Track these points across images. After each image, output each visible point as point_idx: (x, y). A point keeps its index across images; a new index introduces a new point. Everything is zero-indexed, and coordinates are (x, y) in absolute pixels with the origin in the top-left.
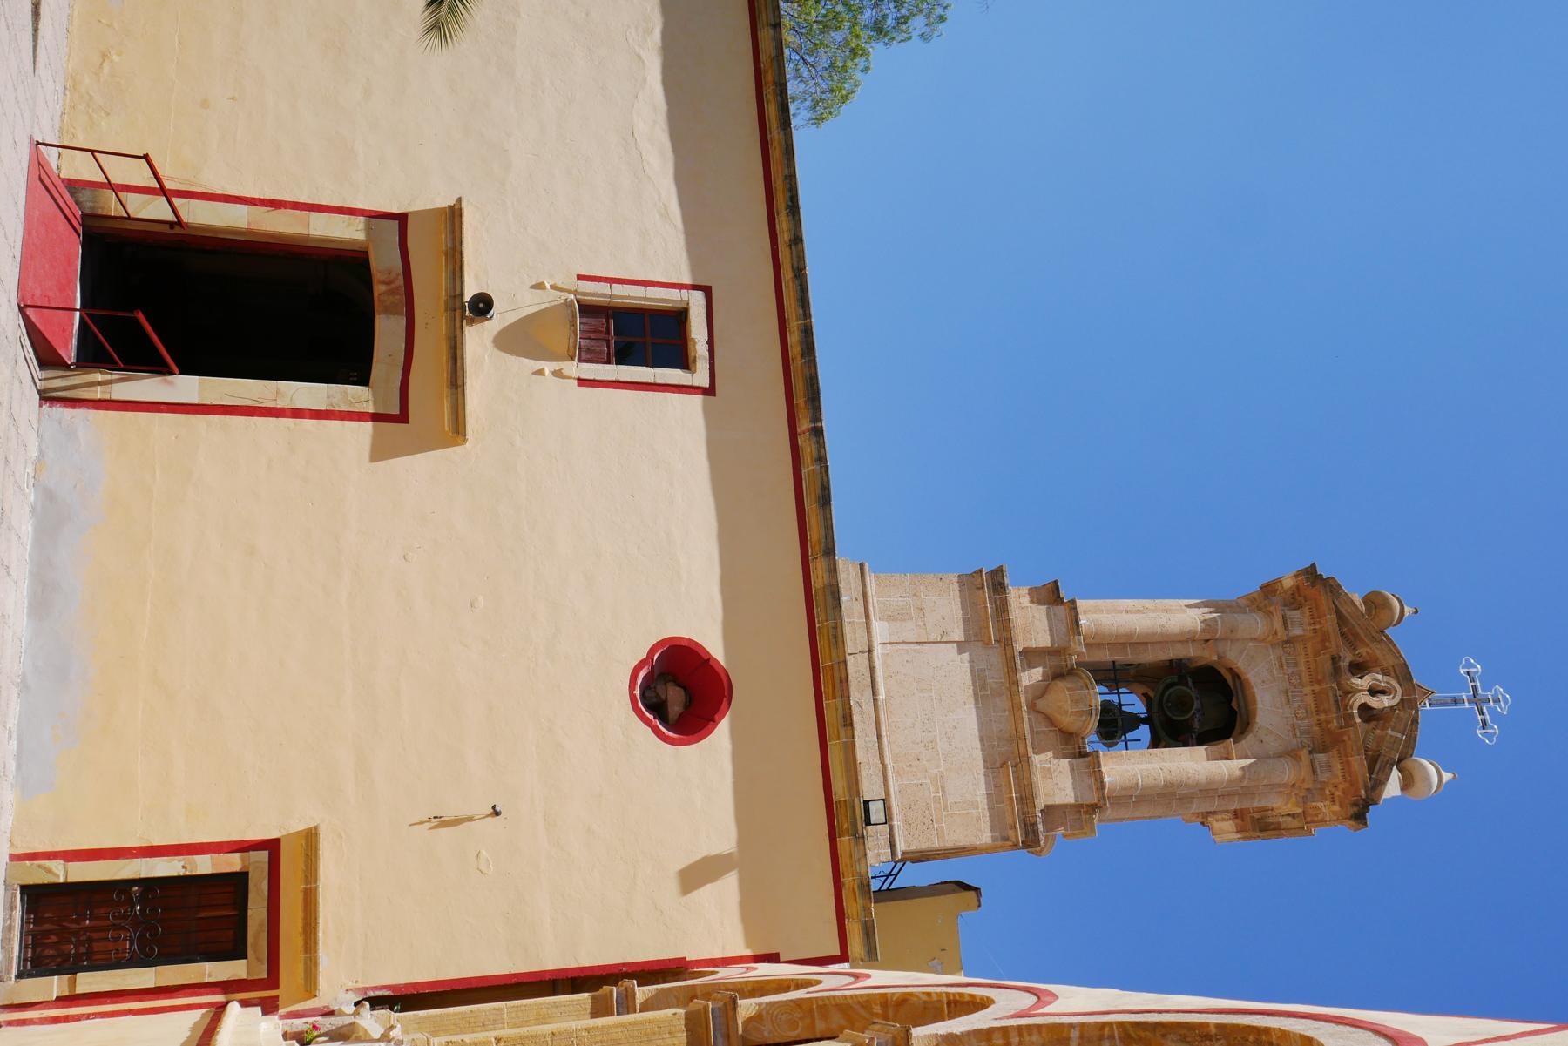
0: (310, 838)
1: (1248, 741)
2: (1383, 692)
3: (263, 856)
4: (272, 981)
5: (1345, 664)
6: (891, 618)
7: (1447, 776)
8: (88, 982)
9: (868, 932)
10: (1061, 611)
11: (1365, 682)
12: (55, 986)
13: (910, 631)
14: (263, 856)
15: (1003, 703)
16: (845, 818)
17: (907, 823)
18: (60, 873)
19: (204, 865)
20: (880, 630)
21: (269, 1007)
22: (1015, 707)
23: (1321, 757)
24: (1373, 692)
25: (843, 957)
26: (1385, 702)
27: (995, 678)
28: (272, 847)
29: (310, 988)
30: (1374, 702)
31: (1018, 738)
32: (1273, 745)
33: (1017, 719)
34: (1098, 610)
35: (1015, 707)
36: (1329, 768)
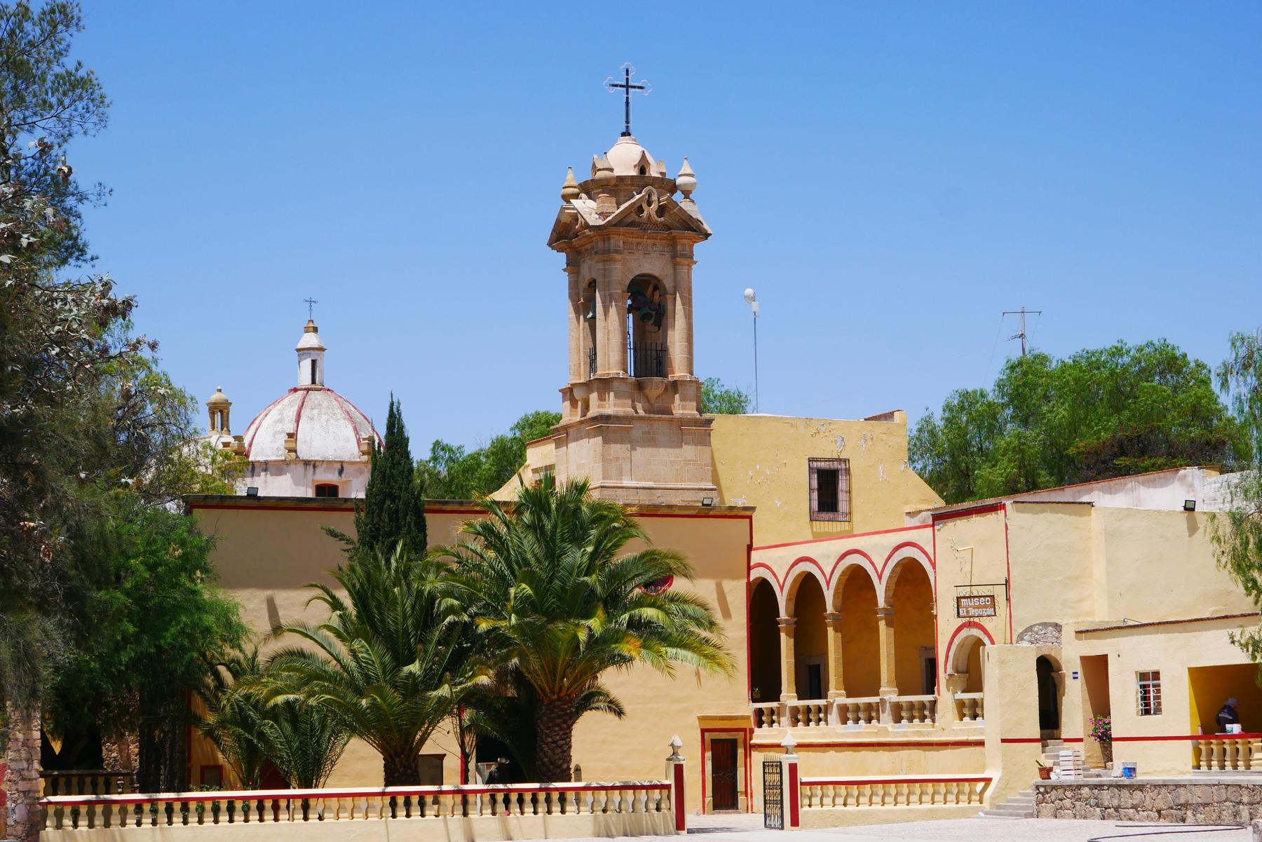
0: (702, 719)
1: (668, 284)
2: (650, 196)
3: (706, 734)
4: (744, 730)
5: (637, 219)
6: (620, 475)
7: (686, 169)
8: (741, 787)
9: (746, 509)
10: (616, 384)
11: (645, 206)
12: (741, 798)
13: (626, 466)
14: (706, 734)
15: (656, 424)
16: (706, 512)
17: (701, 480)
18: (709, 799)
19: (709, 754)
20: (626, 482)
21: (752, 731)
22: (659, 419)
23: (679, 248)
24: (649, 204)
25: (750, 518)
26: (655, 198)
27: (645, 427)
28: (703, 731)
29: (747, 718)
30: (654, 206)
31: (671, 420)
32: (669, 270)
33: (664, 420)
34: (606, 355)
35: (659, 419)
36: (684, 245)
